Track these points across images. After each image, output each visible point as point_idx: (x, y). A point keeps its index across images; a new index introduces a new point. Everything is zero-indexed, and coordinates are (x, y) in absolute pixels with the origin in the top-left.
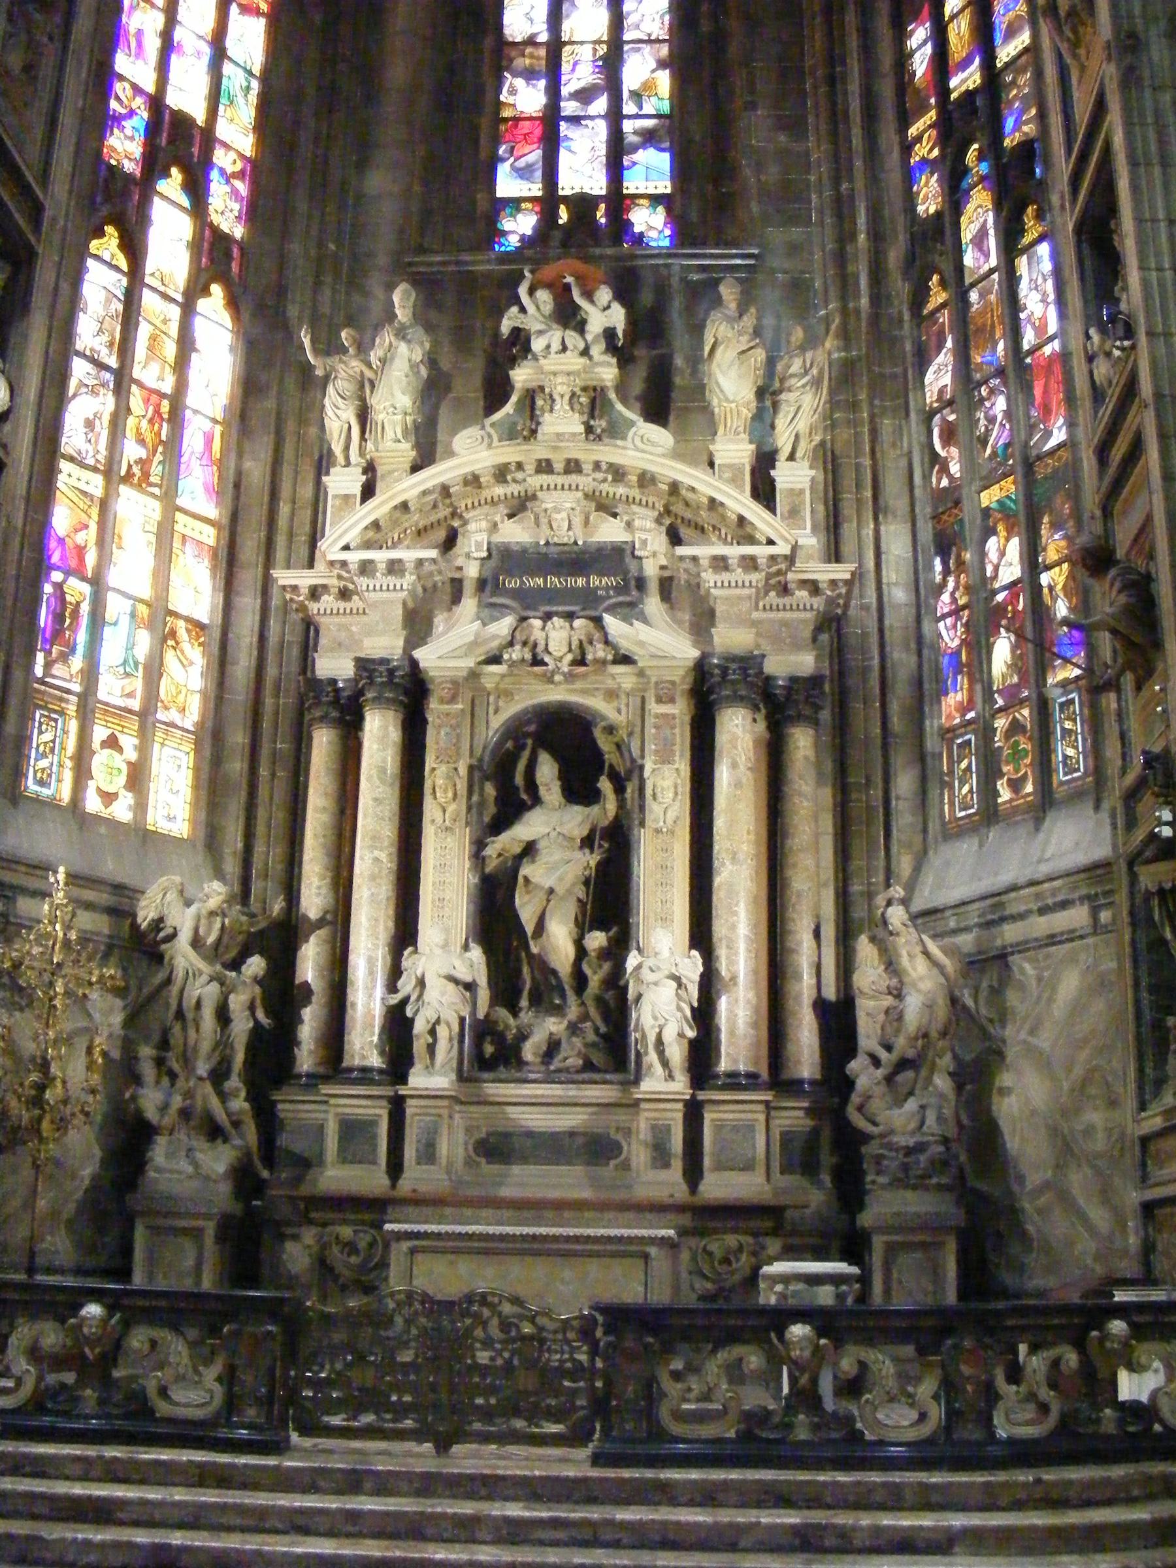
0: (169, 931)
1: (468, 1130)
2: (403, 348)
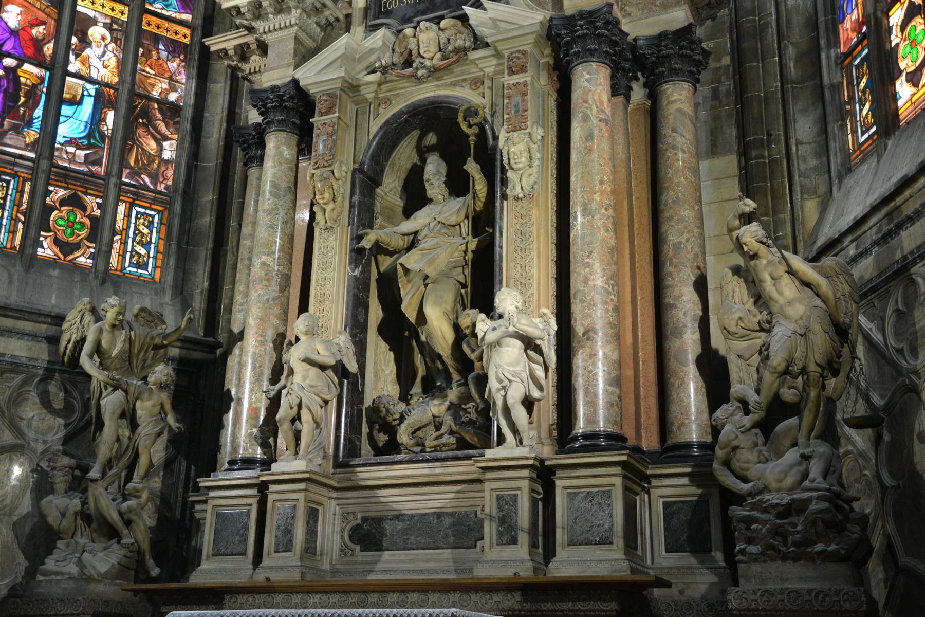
1: (345, 517)
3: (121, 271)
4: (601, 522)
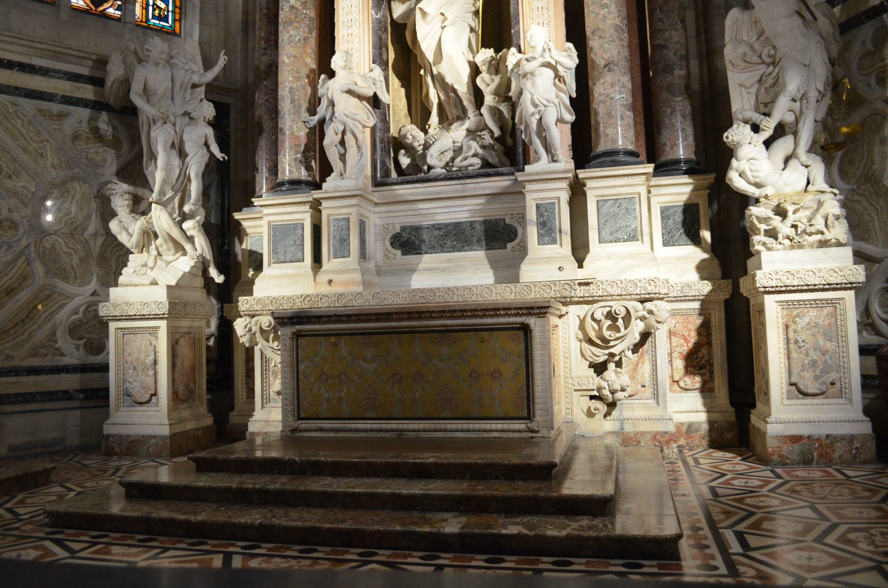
3: (146, 22)
4: (628, 224)
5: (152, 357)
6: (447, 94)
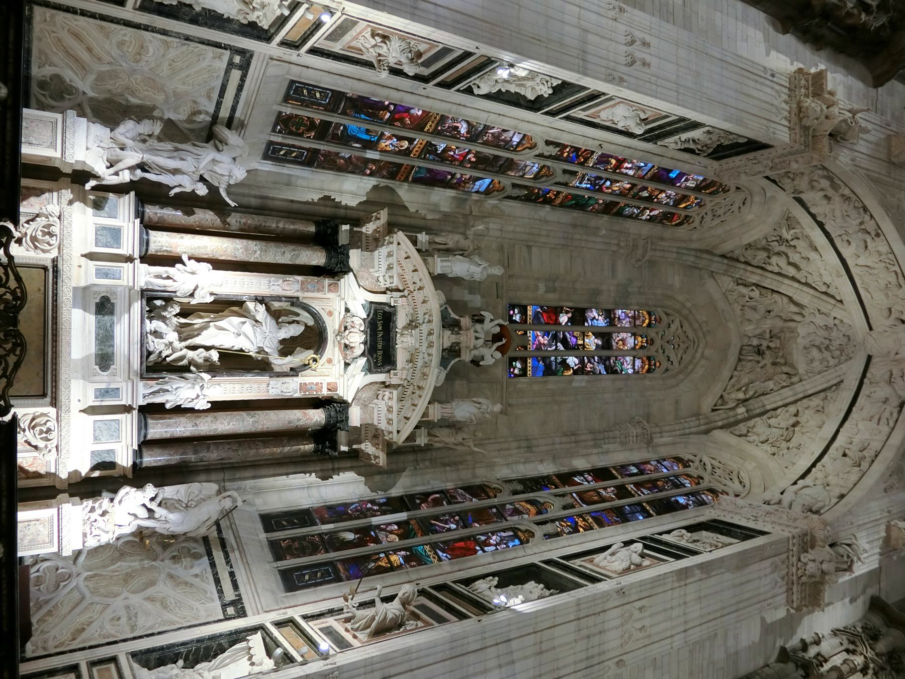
0: (220, 147)
2: (479, 269)
5: (34, 142)
6: (197, 329)
